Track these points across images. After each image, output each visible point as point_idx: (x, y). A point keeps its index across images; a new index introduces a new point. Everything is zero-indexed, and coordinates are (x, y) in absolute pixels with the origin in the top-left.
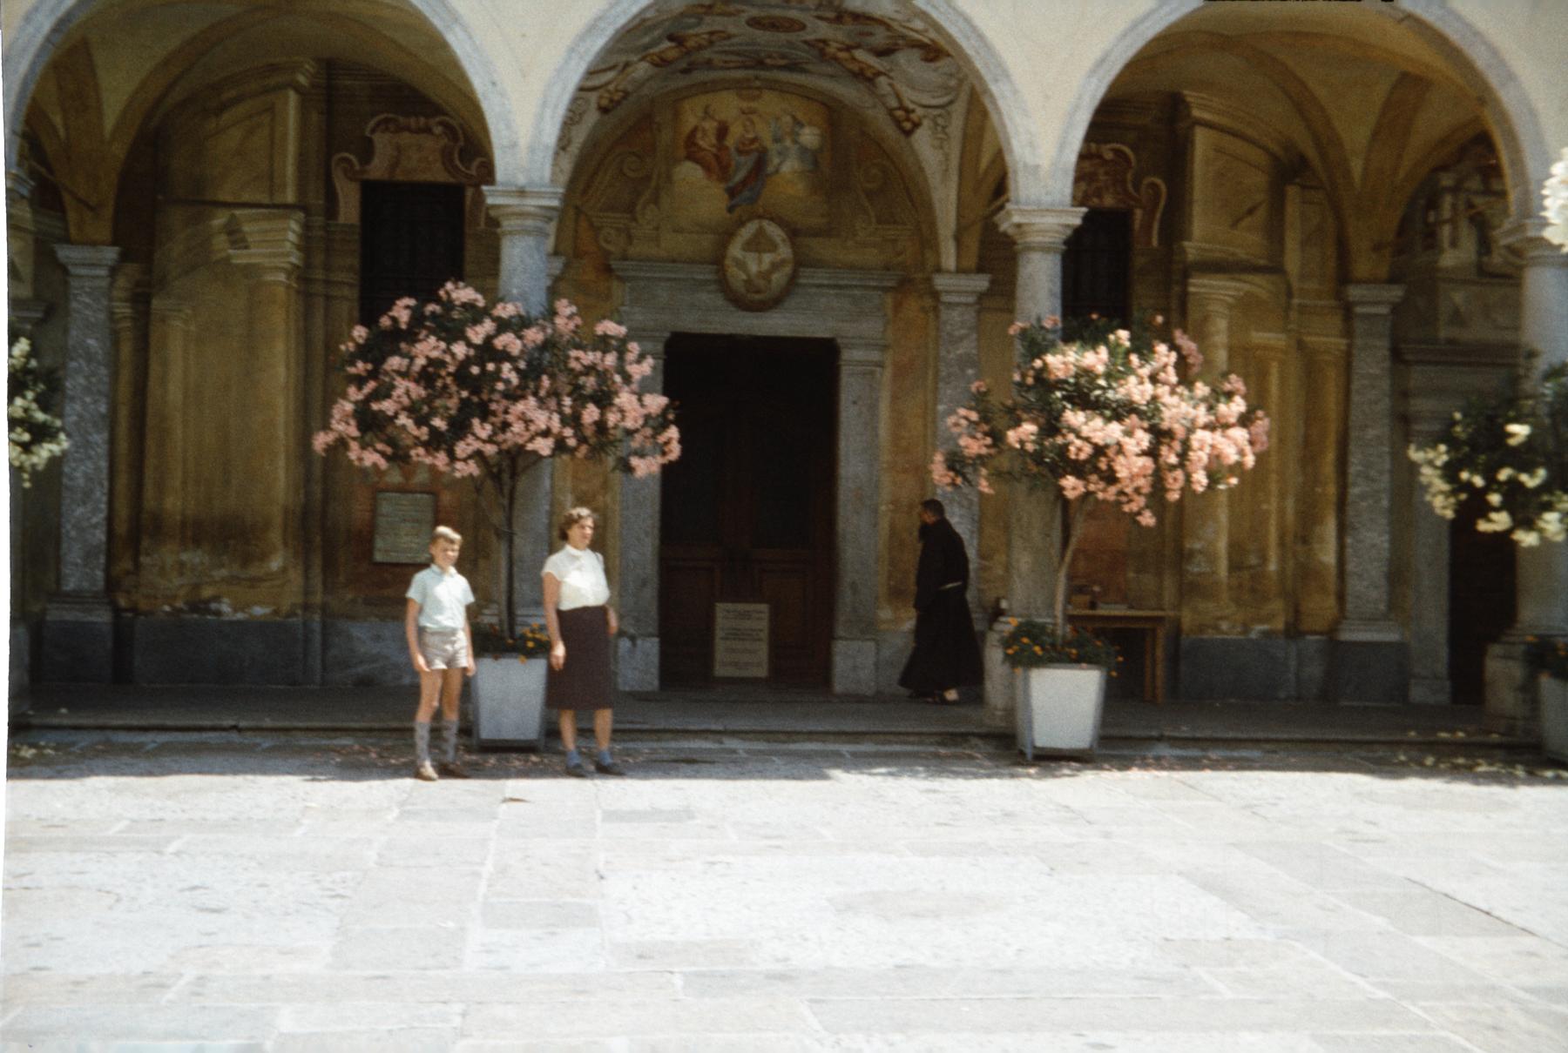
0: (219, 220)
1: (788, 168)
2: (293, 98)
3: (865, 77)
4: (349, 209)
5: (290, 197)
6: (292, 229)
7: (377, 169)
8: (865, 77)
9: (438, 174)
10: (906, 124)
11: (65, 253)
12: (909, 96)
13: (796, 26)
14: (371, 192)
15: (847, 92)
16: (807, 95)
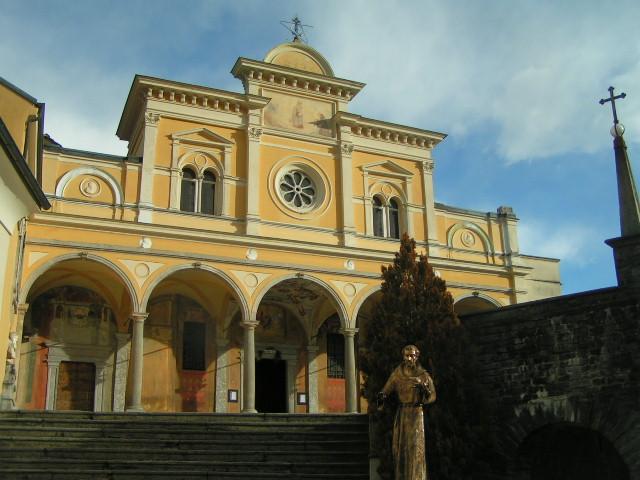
0: (154, 329)
1: (276, 322)
2: (170, 303)
3: (297, 302)
4: (181, 327)
5: (169, 324)
6: (170, 332)
7: (188, 319)
8: (297, 302)
9: (201, 321)
10: (303, 313)
11: (118, 335)
12: (305, 307)
13: (288, 291)
14: (187, 324)
15: (290, 306)
16: (279, 306)
